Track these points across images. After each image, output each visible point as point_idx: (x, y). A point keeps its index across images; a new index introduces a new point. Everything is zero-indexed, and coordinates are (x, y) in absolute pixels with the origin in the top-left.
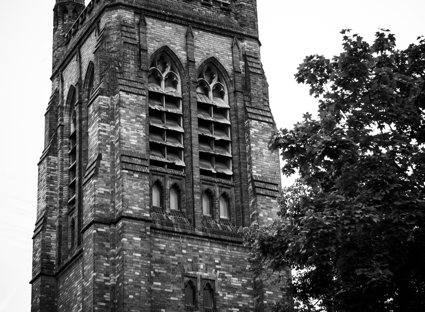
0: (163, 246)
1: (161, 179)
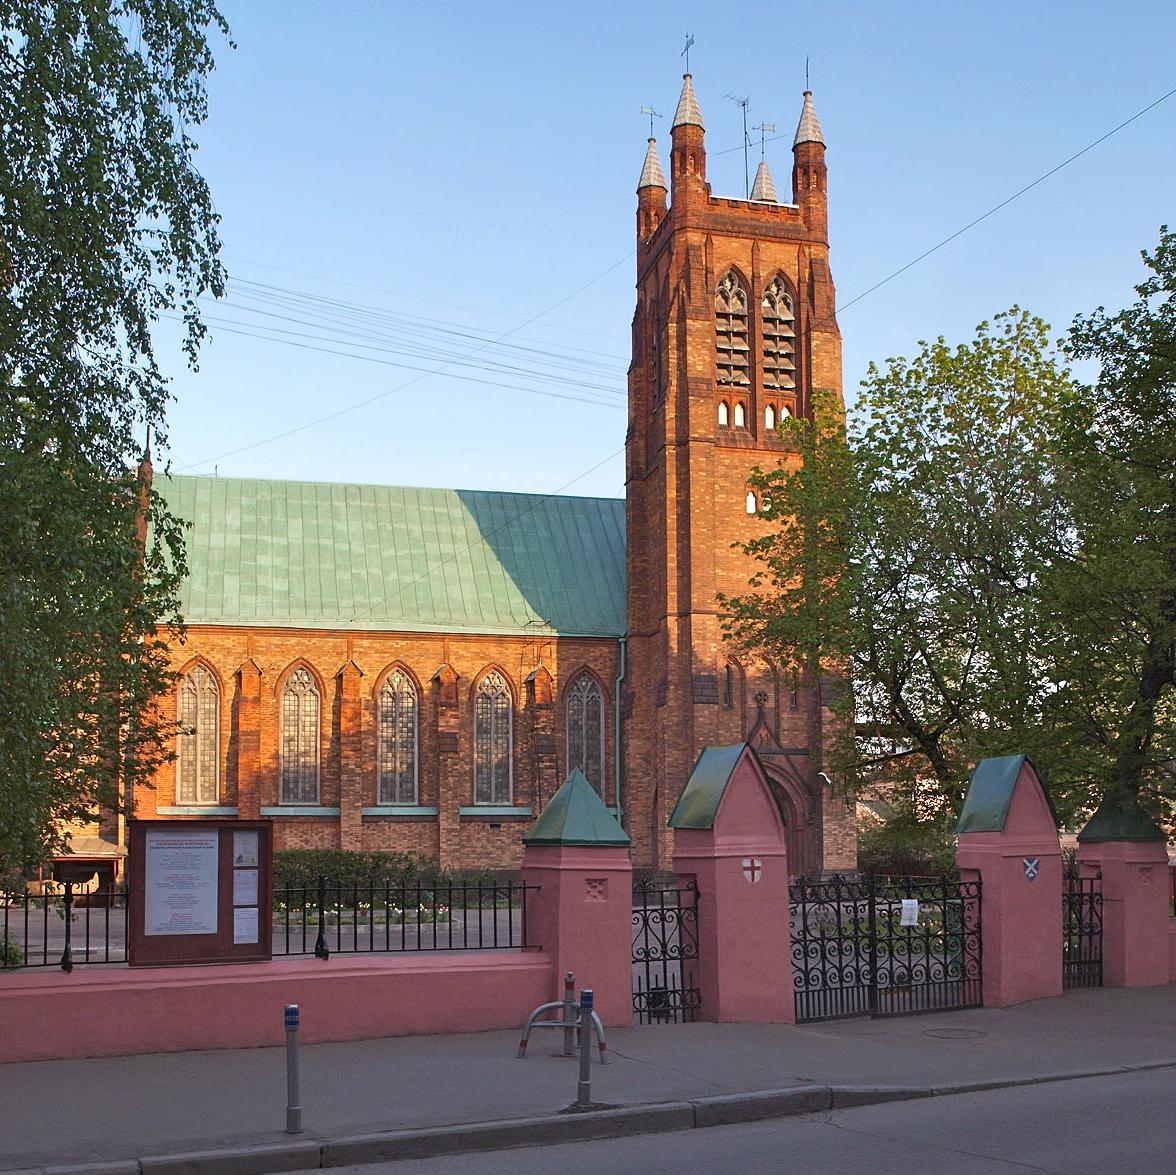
0: (727, 462)
1: (727, 398)
